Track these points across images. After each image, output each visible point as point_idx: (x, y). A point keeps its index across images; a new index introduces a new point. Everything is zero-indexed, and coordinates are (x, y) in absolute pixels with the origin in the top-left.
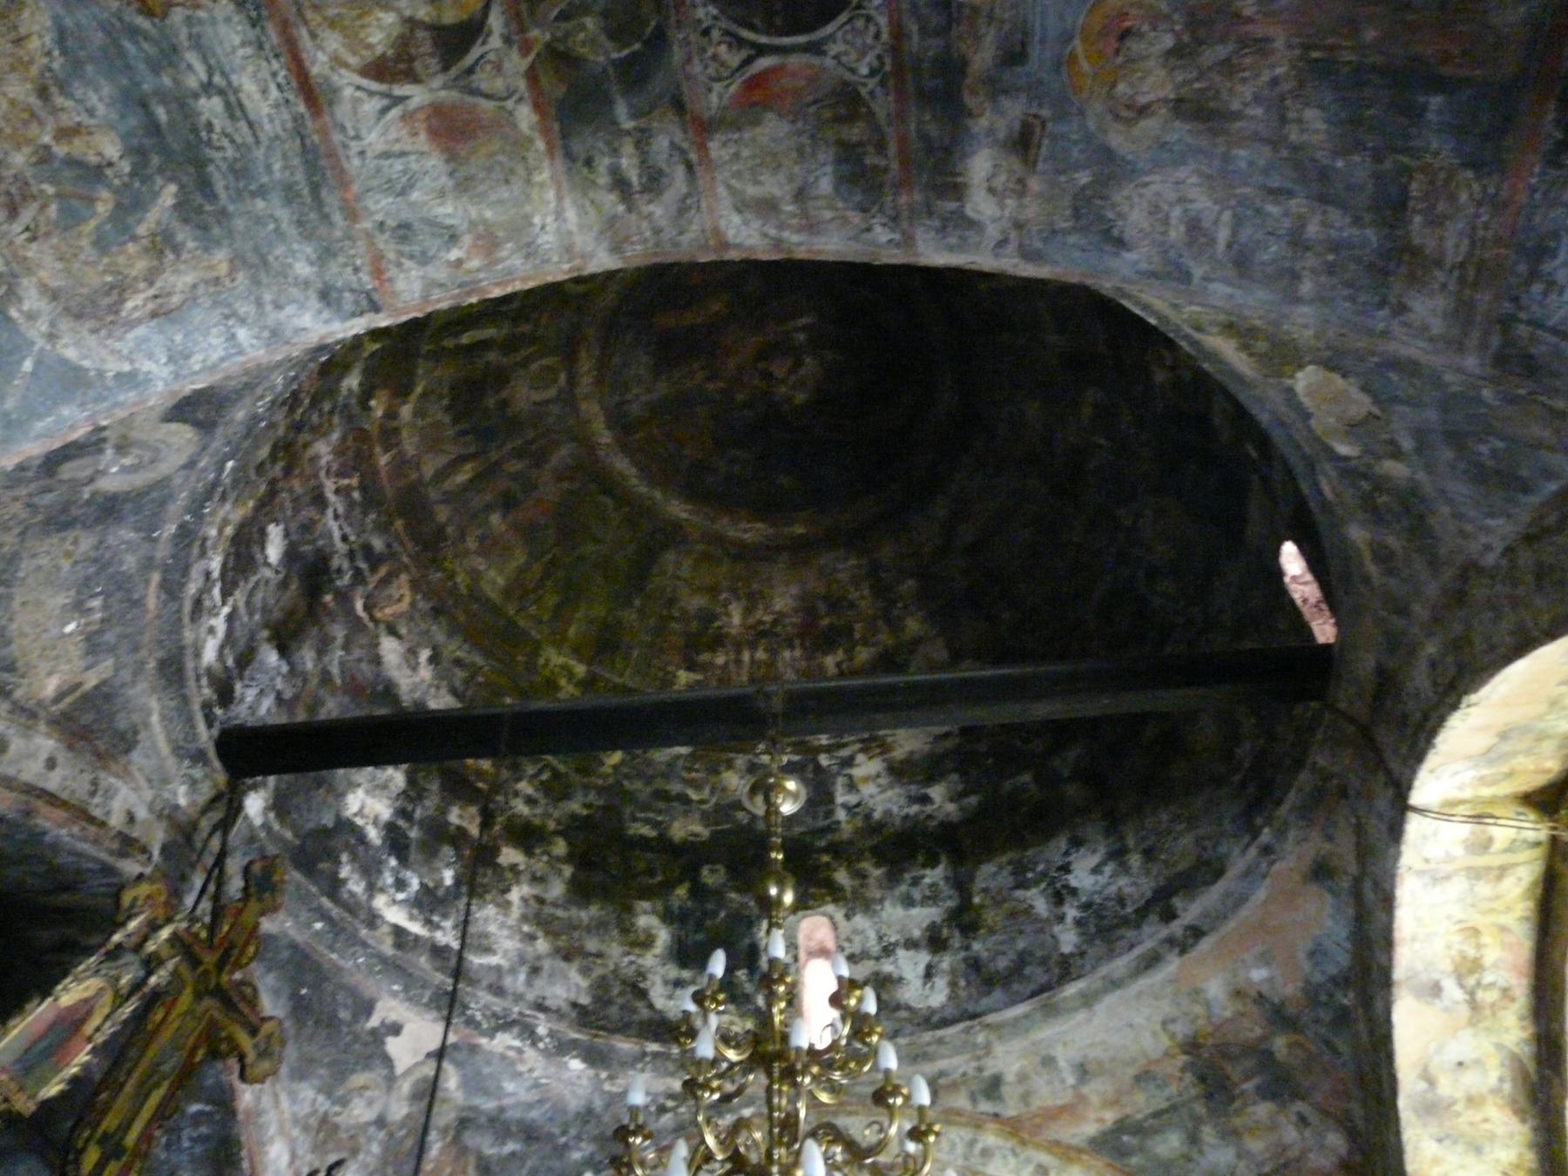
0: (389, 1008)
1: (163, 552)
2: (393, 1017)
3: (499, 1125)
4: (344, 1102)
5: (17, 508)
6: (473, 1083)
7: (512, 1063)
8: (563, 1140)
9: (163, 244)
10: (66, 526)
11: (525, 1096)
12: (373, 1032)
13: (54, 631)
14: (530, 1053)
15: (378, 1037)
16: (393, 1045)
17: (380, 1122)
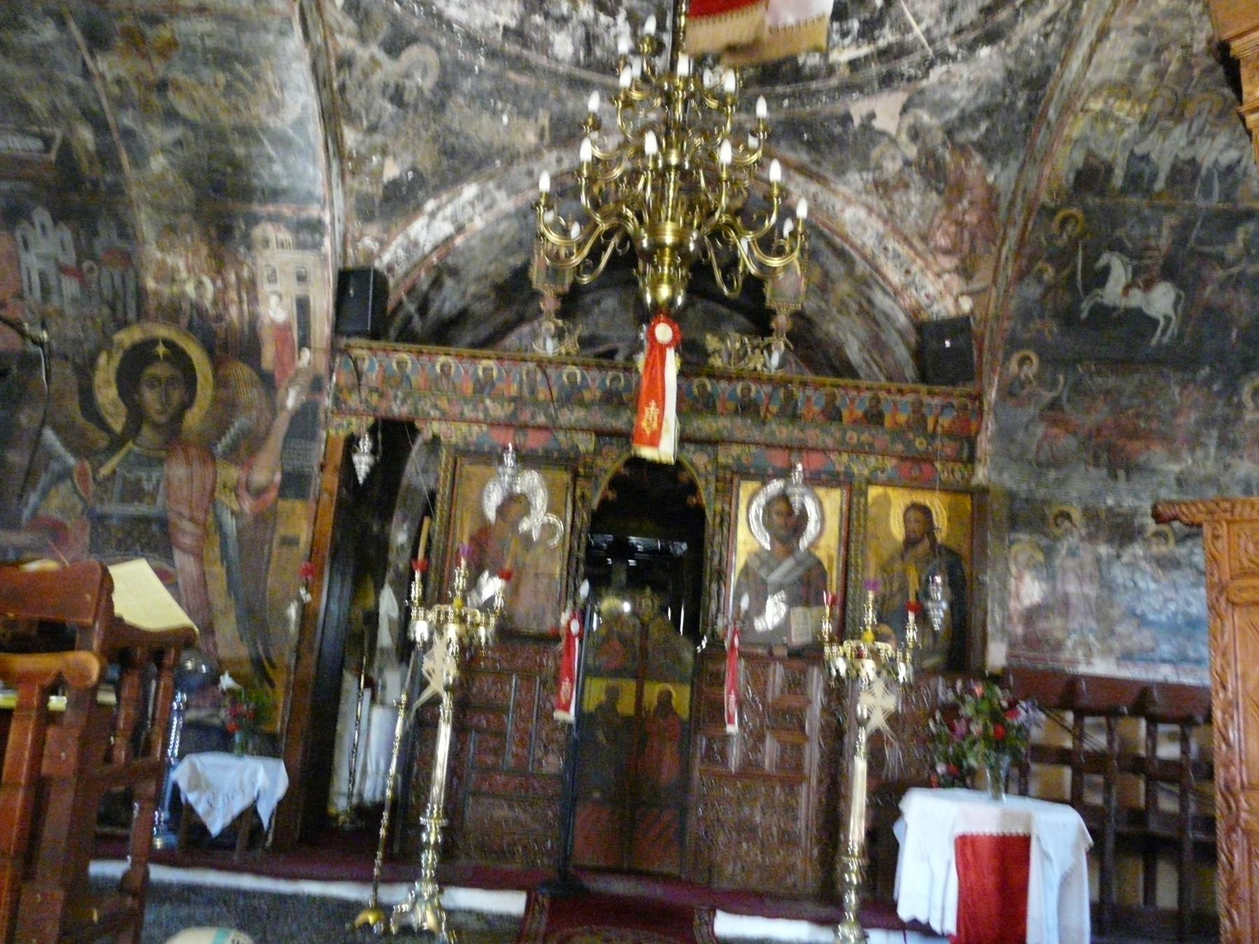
0: (858, 108)
1: (495, 68)
2: (864, 113)
3: (967, 119)
4: (879, 167)
5: (418, 121)
6: (938, 108)
7: (948, 82)
8: (1007, 100)
9: (257, 77)
10: (443, 105)
11: (969, 94)
12: (862, 126)
13: (501, 129)
14: (953, 67)
15: (867, 126)
16: (878, 124)
17: (907, 163)
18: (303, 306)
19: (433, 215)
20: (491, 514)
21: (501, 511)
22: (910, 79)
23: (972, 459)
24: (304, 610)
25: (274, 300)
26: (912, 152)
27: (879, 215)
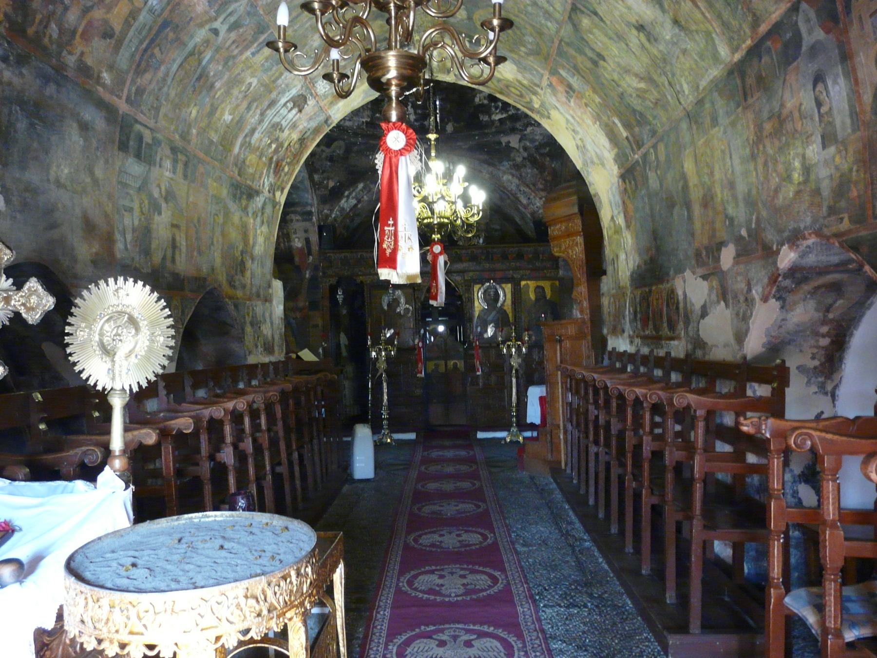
0: (504, 140)
17: (524, 158)
18: (307, 241)
19: (348, 197)
20: (386, 308)
21: (389, 305)
22: (521, 130)
23: (557, 268)
24: (324, 349)
25: (296, 240)
26: (525, 155)
27: (517, 177)
